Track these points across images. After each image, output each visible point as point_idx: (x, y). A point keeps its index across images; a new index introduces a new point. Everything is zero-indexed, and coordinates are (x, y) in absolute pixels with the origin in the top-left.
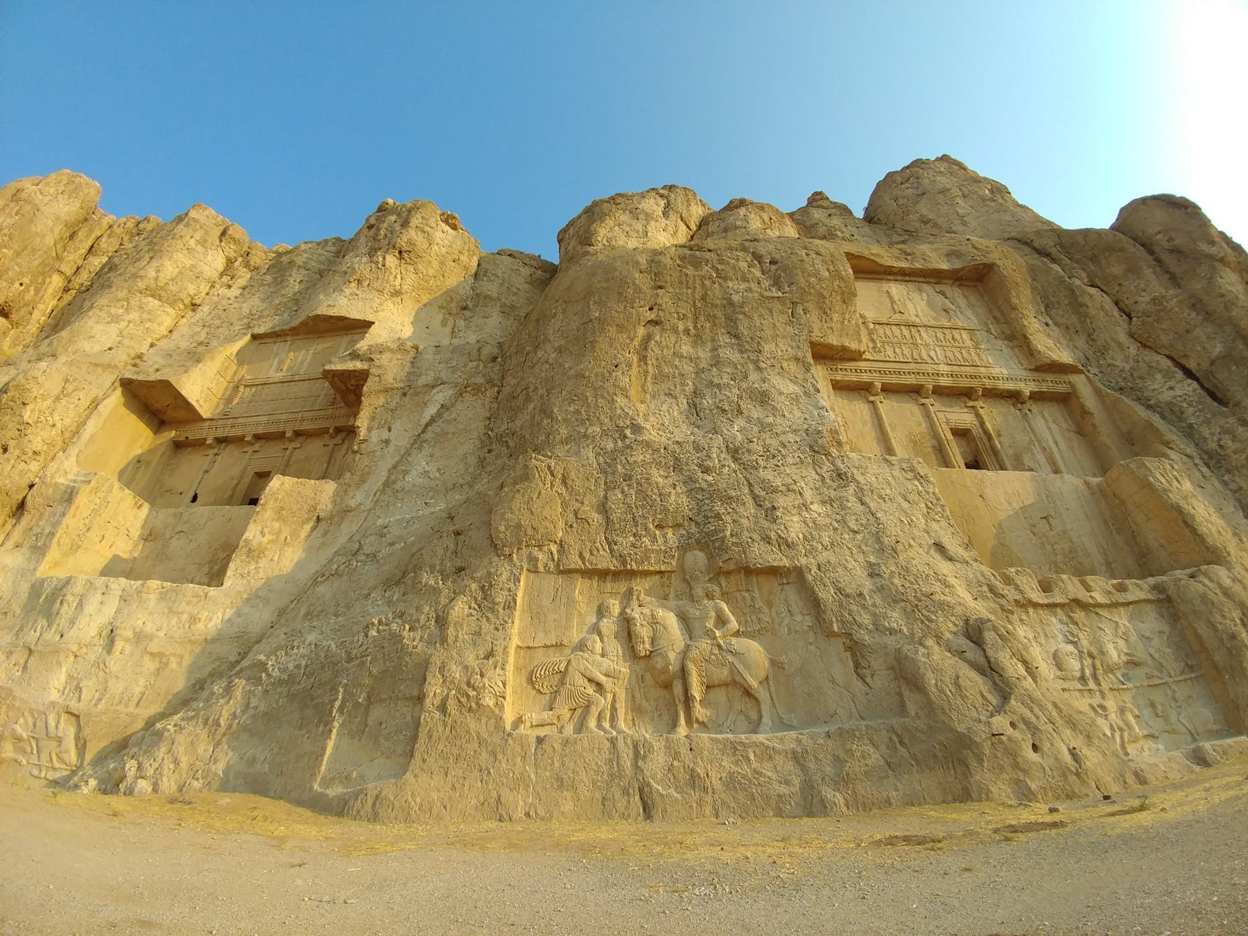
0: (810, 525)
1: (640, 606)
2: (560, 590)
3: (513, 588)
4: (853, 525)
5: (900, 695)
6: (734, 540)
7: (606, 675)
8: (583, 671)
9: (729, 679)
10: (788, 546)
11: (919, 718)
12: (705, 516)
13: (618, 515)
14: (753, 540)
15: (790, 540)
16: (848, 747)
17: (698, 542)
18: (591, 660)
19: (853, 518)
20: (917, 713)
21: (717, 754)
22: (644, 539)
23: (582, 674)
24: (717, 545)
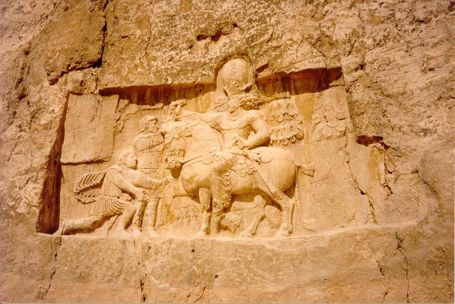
0: (366, 18)
1: (177, 120)
2: (100, 109)
4: (420, 15)
5: (417, 199)
7: (138, 186)
8: (117, 183)
9: (254, 187)
11: (427, 223)
13: (160, 29)
15: (334, 39)
16: (346, 250)
17: (238, 48)
18: (124, 172)
19: (423, 4)
20: (426, 219)
22: (184, 52)
24: (255, 51)
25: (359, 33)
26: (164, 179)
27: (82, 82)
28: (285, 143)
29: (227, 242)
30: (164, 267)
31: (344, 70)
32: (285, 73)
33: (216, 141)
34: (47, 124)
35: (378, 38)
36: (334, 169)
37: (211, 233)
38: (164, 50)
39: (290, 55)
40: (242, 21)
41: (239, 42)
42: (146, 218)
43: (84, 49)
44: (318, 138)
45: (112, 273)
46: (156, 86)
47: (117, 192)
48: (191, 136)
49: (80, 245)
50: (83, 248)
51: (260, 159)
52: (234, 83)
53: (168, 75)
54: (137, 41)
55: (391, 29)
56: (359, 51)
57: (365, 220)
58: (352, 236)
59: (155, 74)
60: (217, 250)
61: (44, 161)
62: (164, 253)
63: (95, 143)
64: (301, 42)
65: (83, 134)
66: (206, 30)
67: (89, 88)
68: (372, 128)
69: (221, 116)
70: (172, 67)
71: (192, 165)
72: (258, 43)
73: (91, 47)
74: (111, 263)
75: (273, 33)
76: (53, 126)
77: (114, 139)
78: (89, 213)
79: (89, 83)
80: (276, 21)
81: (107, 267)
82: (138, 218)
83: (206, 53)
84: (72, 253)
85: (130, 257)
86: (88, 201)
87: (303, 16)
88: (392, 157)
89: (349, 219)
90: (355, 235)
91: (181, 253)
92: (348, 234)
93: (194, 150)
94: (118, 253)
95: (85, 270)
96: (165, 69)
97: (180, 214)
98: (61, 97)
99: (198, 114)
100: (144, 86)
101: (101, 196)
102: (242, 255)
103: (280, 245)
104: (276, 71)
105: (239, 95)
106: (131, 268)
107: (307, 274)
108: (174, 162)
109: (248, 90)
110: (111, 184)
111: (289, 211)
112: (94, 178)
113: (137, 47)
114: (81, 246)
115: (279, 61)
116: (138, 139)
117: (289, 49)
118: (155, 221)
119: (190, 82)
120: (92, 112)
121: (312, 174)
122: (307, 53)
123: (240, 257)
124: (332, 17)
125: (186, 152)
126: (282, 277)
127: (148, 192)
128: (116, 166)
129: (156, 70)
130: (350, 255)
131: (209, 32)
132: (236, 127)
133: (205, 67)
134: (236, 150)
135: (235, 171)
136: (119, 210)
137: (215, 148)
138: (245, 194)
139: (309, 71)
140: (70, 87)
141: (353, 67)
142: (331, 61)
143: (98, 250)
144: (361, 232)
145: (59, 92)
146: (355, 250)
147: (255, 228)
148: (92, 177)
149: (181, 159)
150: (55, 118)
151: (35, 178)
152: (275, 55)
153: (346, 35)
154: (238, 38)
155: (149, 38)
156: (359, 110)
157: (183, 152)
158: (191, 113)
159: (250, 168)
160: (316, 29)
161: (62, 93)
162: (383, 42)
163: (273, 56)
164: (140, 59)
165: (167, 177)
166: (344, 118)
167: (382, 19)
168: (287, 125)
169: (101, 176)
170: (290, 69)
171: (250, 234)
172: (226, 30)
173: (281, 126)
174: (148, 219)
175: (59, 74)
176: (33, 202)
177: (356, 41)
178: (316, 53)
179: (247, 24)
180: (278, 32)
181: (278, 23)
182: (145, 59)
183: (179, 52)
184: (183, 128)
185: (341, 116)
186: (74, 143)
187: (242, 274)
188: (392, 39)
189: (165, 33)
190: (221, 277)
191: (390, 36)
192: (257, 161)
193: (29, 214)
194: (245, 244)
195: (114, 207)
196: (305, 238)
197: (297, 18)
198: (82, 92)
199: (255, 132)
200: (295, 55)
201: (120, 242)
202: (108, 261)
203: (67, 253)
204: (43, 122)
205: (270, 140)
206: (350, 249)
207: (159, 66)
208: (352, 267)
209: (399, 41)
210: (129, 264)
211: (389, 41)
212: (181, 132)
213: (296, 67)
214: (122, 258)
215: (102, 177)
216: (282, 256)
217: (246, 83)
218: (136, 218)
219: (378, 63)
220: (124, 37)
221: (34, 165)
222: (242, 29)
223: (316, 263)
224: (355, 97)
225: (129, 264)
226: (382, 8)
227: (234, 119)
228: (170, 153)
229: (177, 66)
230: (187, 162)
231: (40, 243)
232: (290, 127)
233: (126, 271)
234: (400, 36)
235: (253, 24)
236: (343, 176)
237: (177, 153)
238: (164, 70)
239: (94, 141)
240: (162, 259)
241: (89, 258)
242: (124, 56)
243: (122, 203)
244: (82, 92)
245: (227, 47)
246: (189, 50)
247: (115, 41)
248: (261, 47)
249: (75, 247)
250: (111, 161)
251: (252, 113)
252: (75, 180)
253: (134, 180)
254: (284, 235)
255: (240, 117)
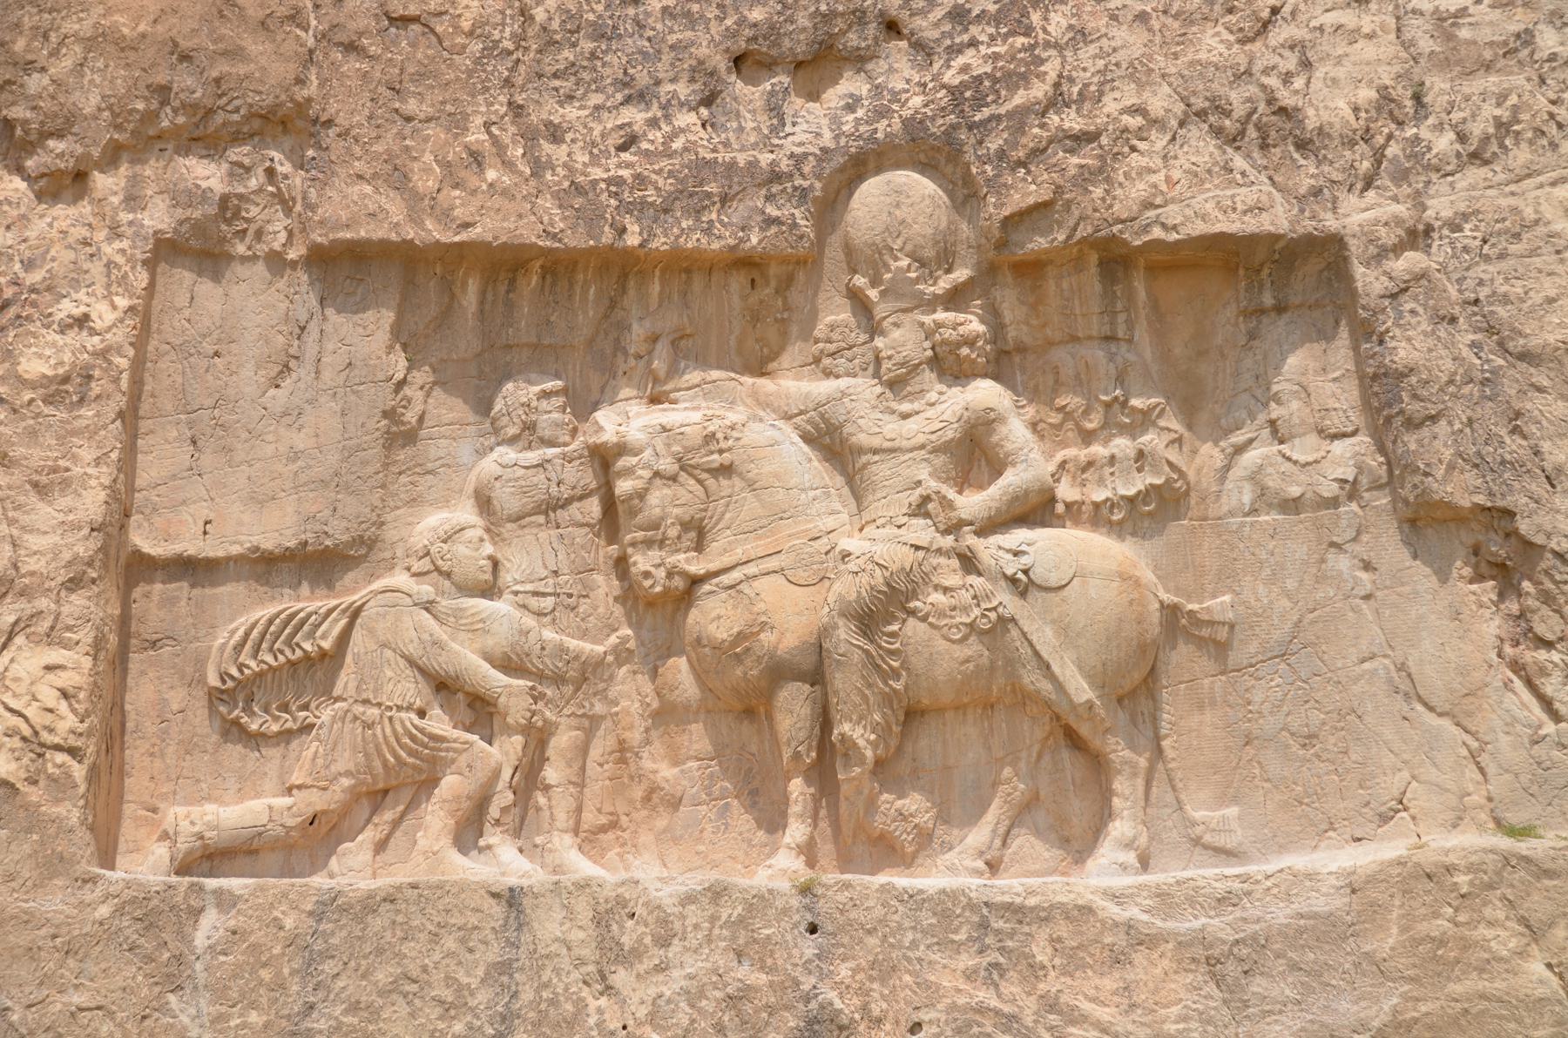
0: (1426, 45)
1: (655, 400)
2: (313, 328)
3: (103, 315)
6: (1072, 121)
7: (509, 665)
8: (413, 650)
10: (1302, 145)
12: (959, 16)
14: (1155, 122)
15: (1311, 123)
16: (1423, 928)
17: (914, 126)
18: (444, 603)
21: (914, 944)
22: (685, 119)
23: (412, 663)
24: (993, 144)
25: (1401, 106)
26: (613, 639)
27: (224, 199)
28: (1117, 517)
29: (944, 891)
30: (702, 994)
31: (1353, 249)
32: (1125, 243)
33: (828, 495)
34: (66, 379)
35: (1477, 129)
36: (1313, 622)
37: (823, 862)
38: (596, 99)
39: (1139, 174)
40: (923, 13)
41: (917, 101)
42: (541, 800)
43: (225, 53)
44: (1247, 498)
45: (470, 1027)
46: (568, 250)
47: (408, 689)
48: (726, 470)
49: (311, 914)
50: (326, 926)
51: (1026, 572)
52: (905, 262)
53: (626, 208)
54: (464, 47)
55: (1524, 98)
56: (1402, 176)
57: (1451, 815)
58: (1435, 875)
59: (561, 198)
60: (907, 924)
61: (85, 547)
62: (694, 939)
63: (303, 478)
64: (1182, 124)
65: (245, 435)
66: (772, 31)
67: (259, 234)
68: (1471, 478)
69: (844, 394)
70: (637, 176)
71: (744, 587)
72: (1002, 111)
73: (255, 46)
74: (460, 989)
75: (1060, 76)
76: (95, 388)
77: (386, 466)
78: (283, 773)
79: (254, 211)
80: (1071, 27)
81: (442, 1002)
82: (510, 797)
83: (774, 130)
84: (275, 951)
85: (547, 956)
86: (275, 728)
87: (1176, 17)
88: (1549, 585)
89: (1383, 809)
90: (1450, 869)
91: (768, 937)
92: (1418, 864)
93: (745, 528)
94: (486, 943)
95: (348, 1020)
96: (609, 181)
97: (685, 783)
98: (120, 259)
99: (748, 380)
100: (524, 245)
101: (338, 705)
102: (1010, 944)
103: (1147, 902)
104: (1084, 231)
105: (923, 313)
106: (553, 1002)
107: (1281, 1012)
108: (661, 574)
109: (955, 299)
110: (388, 653)
111: (1135, 775)
112: (306, 628)
113: (470, 73)
114: (318, 915)
115: (1098, 192)
116: (499, 471)
117: (1133, 149)
118: (579, 810)
119: (716, 246)
120: (281, 339)
121: (1222, 633)
122: (1209, 171)
123: (1002, 950)
124: (1298, 33)
125: (709, 537)
126: (1181, 1026)
127: (549, 692)
128: (400, 579)
129: (566, 184)
130: (1442, 942)
131: (787, 43)
132: (921, 439)
133: (775, 189)
134: (921, 531)
135: (924, 619)
136: (424, 765)
137: (830, 522)
138: (957, 708)
139: (1222, 234)
140: (158, 217)
141: (1388, 237)
142: (1302, 211)
143: (399, 934)
144: (1474, 858)
145: (101, 235)
146: (1456, 925)
147: (998, 842)
148: (295, 624)
149: (687, 561)
150: (103, 354)
151: (47, 624)
152: (1082, 166)
153: (1356, 110)
154: (908, 81)
155: (519, 39)
156: (1417, 406)
157: (698, 533)
158: (715, 374)
159: (984, 606)
160: (1238, 77)
161: (125, 244)
162: (1494, 147)
163: (1073, 171)
164: (487, 125)
165: (620, 633)
166: (1350, 429)
167: (1488, 54)
168: (1122, 445)
169: (336, 621)
170: (1146, 229)
171: (980, 864)
172: (855, 44)
173: (1098, 450)
174: (557, 804)
175: (96, 153)
176: (51, 730)
177: (1390, 137)
178: (1243, 174)
179: (947, 27)
180: (1082, 74)
181: (1080, 35)
182: (512, 129)
183: (659, 114)
184: (694, 434)
185: (1335, 422)
186: (195, 471)
187: (1013, 1018)
188: (1530, 134)
189: (594, 24)
190: (935, 1029)
191: (1518, 122)
192: (1013, 581)
193: (35, 782)
194: (1018, 900)
195: (403, 754)
196: (1245, 879)
197: (1156, 24)
198: (227, 247)
199: (997, 470)
200: (1159, 178)
201: (495, 895)
202: (447, 977)
203: (255, 948)
204: (33, 366)
205: (1053, 500)
206: (1439, 922)
207: (579, 166)
208: (1457, 988)
209: (1554, 146)
210: (546, 986)
211: (1517, 144)
212: (688, 450)
213: (1170, 222)
214: (510, 962)
215: (344, 622)
216: (1170, 946)
217: (948, 271)
218: (503, 797)
219: (1476, 229)
220: (406, 20)
221: (32, 564)
222: (919, 46)
223: (1308, 974)
224: (1402, 353)
225: (546, 986)
226: (1483, 7)
227: (906, 407)
228: (640, 535)
229: (659, 172)
230: (717, 574)
231: (119, 911)
232: (1132, 454)
233: (532, 1014)
234: (1560, 126)
235: (974, 30)
236: (1354, 650)
237: (673, 532)
238: (603, 185)
239: (294, 467)
240: (688, 965)
241: (359, 965)
242: (412, 106)
243: (441, 733)
244: (227, 247)
245: (860, 113)
246: (704, 112)
247: (361, 34)
248: (1021, 129)
249: (289, 923)
250: (373, 557)
251: (985, 392)
252: (215, 638)
253: (490, 642)
254: (1124, 867)
255: (932, 405)
